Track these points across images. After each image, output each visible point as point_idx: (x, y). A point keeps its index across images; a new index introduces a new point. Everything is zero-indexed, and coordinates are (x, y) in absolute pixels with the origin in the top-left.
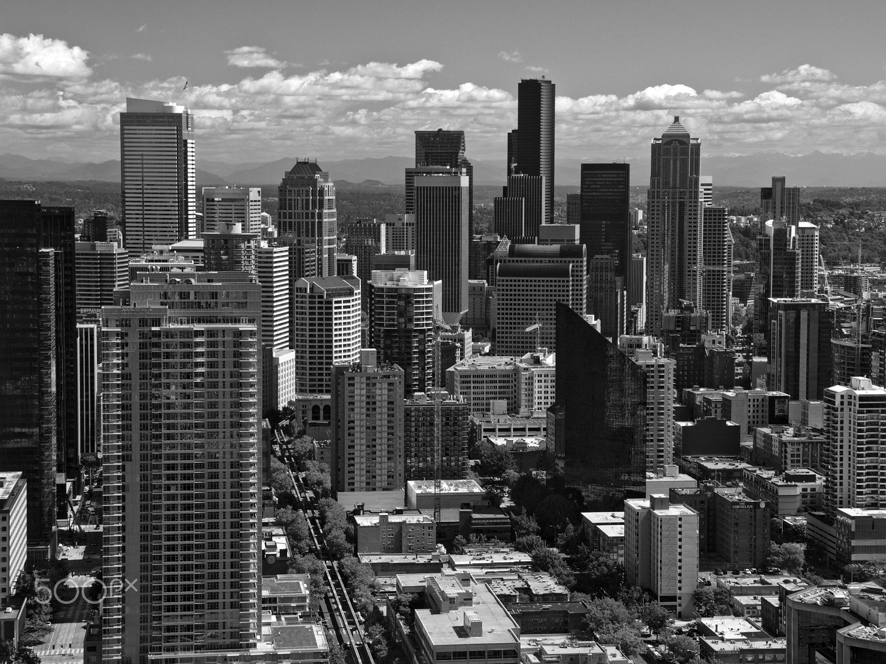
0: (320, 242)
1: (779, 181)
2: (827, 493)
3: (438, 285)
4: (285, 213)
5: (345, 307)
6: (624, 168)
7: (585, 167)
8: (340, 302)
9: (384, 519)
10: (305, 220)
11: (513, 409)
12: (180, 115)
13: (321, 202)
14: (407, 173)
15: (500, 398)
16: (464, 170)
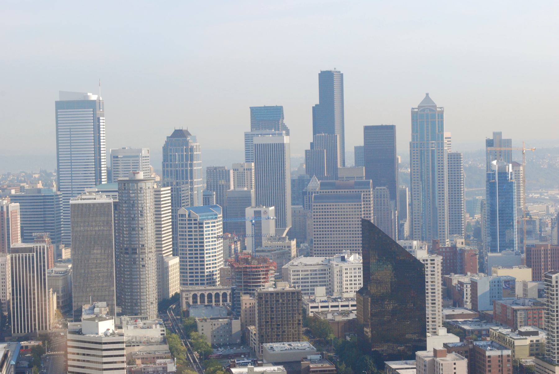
0: (192, 183)
1: (498, 135)
2: (548, 343)
3: (272, 210)
4: (167, 165)
5: (212, 226)
6: (391, 129)
7: (367, 128)
8: (209, 223)
9: (251, 370)
10: (181, 169)
11: (330, 292)
12: (94, 102)
13: (192, 156)
14: (245, 135)
15: (321, 286)
16: (284, 132)
